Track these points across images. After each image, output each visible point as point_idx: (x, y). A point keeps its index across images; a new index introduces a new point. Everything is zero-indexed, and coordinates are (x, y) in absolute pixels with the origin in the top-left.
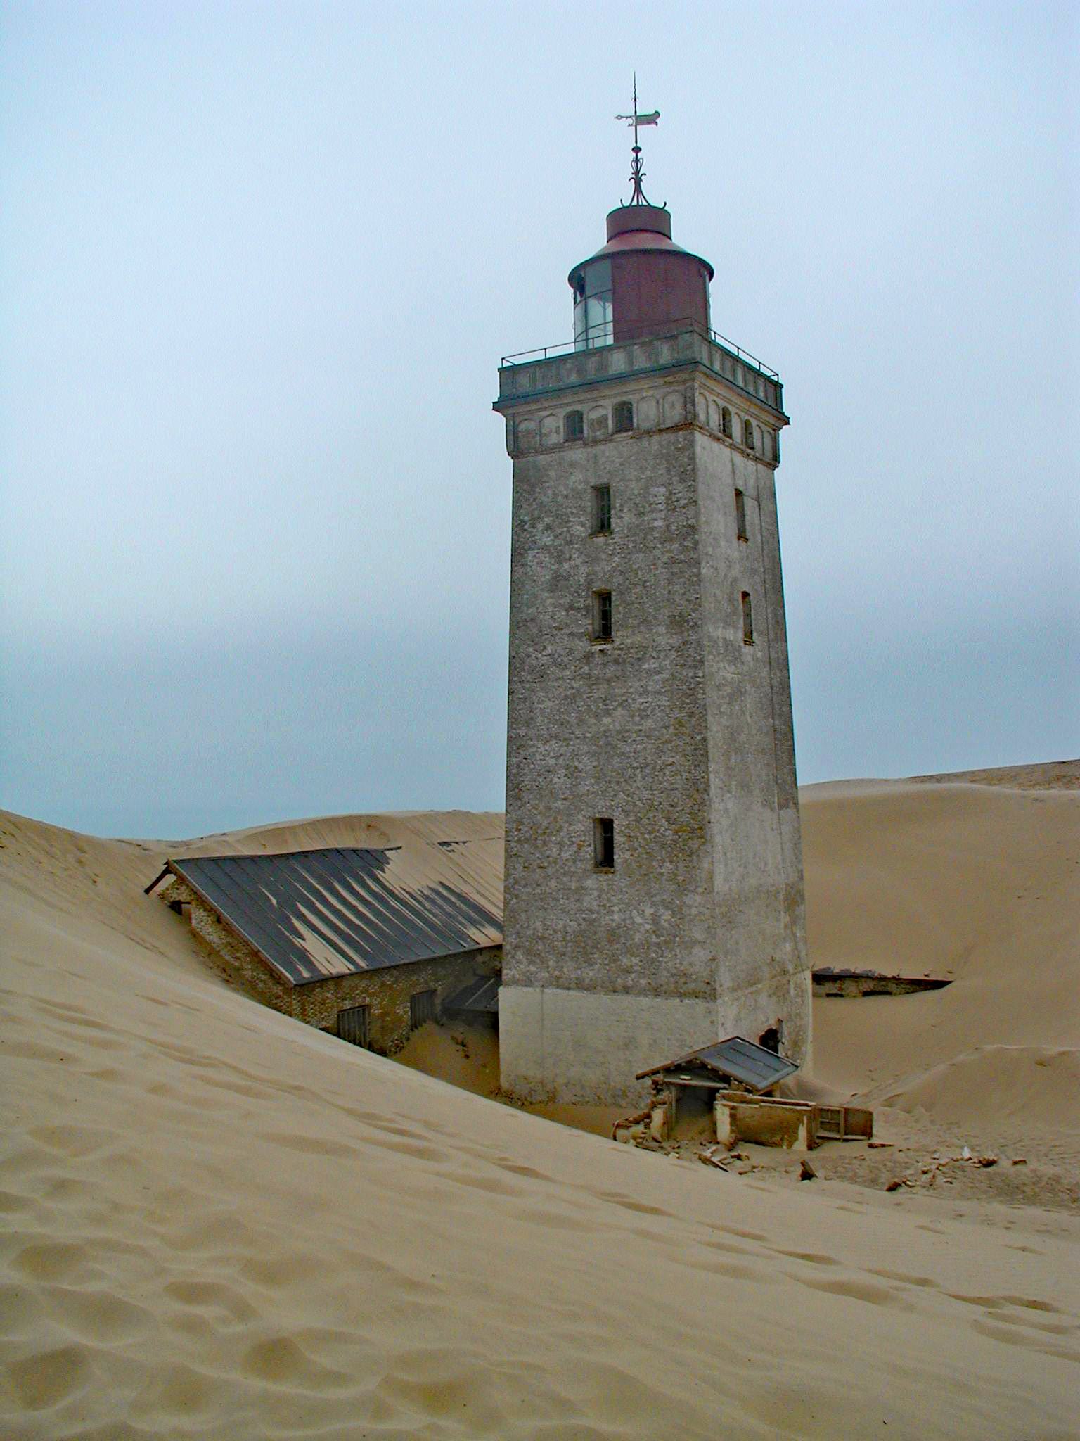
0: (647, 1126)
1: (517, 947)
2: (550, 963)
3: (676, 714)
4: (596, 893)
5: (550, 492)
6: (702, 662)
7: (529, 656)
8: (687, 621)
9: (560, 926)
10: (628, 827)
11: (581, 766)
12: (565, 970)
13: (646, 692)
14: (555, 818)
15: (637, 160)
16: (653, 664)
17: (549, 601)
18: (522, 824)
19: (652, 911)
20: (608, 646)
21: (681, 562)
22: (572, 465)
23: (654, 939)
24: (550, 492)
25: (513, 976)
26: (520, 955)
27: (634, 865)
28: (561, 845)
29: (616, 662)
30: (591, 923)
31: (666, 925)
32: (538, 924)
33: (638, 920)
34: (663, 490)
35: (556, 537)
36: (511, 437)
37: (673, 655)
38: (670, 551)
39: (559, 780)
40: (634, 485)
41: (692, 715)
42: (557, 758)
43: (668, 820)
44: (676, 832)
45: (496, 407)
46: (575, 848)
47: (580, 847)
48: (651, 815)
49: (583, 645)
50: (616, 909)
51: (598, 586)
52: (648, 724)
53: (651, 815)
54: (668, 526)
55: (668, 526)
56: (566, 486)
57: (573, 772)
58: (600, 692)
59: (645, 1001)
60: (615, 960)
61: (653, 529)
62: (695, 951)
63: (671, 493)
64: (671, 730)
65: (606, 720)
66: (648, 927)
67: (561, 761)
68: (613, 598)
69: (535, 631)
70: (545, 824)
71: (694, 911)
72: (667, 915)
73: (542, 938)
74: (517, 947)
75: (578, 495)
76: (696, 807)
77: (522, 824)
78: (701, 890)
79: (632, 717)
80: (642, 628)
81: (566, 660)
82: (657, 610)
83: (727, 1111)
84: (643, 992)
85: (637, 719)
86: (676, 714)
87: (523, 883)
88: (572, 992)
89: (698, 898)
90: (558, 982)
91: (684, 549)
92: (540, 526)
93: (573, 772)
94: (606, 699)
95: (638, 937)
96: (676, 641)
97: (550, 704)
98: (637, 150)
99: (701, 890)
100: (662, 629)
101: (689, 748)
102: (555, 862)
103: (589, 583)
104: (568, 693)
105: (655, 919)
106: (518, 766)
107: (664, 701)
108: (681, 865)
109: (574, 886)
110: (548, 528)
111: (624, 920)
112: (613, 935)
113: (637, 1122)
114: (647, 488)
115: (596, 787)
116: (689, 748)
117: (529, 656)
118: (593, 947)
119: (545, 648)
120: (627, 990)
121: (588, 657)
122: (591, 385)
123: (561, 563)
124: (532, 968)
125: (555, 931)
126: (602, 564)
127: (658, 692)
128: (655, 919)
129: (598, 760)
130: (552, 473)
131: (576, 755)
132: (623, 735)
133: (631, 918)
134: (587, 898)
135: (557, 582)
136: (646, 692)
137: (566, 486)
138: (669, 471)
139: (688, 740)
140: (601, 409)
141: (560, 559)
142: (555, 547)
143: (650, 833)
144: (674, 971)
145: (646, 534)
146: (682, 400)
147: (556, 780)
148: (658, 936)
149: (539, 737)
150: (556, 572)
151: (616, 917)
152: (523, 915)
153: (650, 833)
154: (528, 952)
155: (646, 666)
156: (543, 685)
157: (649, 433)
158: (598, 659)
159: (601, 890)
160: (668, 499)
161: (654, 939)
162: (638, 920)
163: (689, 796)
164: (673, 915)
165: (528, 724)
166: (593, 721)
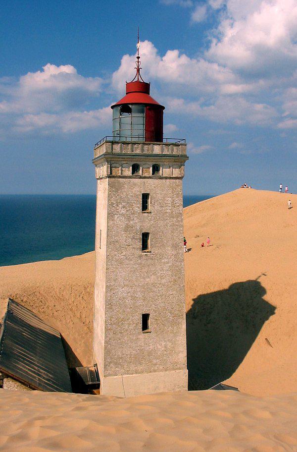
3: (174, 277)
4: (143, 340)
5: (125, 193)
6: (183, 260)
9: (129, 352)
15: (138, 62)
16: (166, 260)
21: (177, 225)
22: (135, 184)
23: (165, 352)
24: (125, 193)
25: (109, 373)
28: (129, 324)
30: (141, 350)
32: (119, 353)
33: (159, 347)
34: (170, 199)
35: (127, 211)
36: (109, 169)
37: (173, 257)
39: (128, 302)
41: (179, 278)
43: (171, 313)
44: (173, 317)
49: (139, 252)
52: (163, 281)
54: (172, 212)
55: (172, 212)
56: (132, 192)
57: (134, 298)
58: (146, 270)
59: (162, 373)
60: (150, 361)
65: (148, 280)
66: (163, 349)
67: (129, 294)
70: (122, 317)
72: (169, 344)
73: (121, 358)
75: (136, 196)
79: (158, 278)
84: (161, 371)
86: (174, 277)
88: (134, 375)
89: (181, 337)
90: (128, 373)
91: (178, 221)
92: (120, 206)
93: (134, 298)
96: (174, 252)
103: (141, 230)
105: (166, 347)
106: (111, 296)
107: (170, 273)
110: (124, 207)
112: (150, 354)
114: (164, 198)
120: (155, 371)
121: (140, 257)
124: (117, 369)
126: (146, 223)
128: (166, 347)
130: (126, 186)
132: (154, 285)
133: (157, 347)
135: (127, 228)
137: (132, 192)
138: (173, 193)
139: (178, 286)
141: (129, 219)
142: (127, 215)
143: (164, 317)
145: (164, 214)
149: (119, 286)
150: (127, 224)
154: (116, 364)
157: (166, 178)
162: (159, 347)
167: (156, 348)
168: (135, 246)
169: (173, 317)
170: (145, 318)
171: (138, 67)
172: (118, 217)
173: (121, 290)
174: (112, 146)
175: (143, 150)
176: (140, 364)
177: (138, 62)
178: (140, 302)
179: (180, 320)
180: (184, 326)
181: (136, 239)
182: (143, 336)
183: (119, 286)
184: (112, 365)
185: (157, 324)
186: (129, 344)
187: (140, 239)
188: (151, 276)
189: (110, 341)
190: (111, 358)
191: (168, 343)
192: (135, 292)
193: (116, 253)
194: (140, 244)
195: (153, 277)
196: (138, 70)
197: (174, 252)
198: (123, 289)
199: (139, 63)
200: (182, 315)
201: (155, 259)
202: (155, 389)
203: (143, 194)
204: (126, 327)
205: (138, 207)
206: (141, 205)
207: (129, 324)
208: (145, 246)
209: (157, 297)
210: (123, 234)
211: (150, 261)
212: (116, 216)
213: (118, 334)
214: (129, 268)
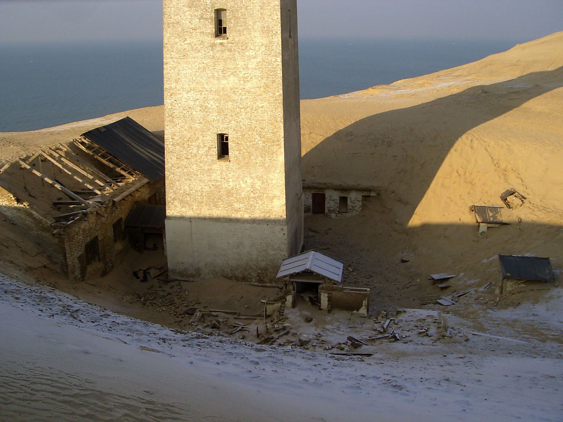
0: (283, 303)
1: (174, 199)
2: (194, 207)
4: (219, 172)
7: (176, 44)
9: (199, 188)
10: (237, 138)
11: (209, 106)
12: (202, 210)
14: (195, 133)
17: (187, 13)
18: (175, 135)
19: (251, 181)
20: (225, 41)
23: (252, 195)
26: (176, 203)
27: (241, 158)
28: (199, 147)
29: (231, 51)
30: (217, 187)
31: (259, 188)
32: (186, 187)
33: (243, 185)
37: (263, 48)
39: (197, 114)
43: (260, 136)
44: (264, 142)
46: (206, 149)
47: (210, 148)
48: (250, 133)
49: (210, 39)
50: (231, 180)
51: (217, 7)
52: (248, 86)
53: (250, 133)
57: (204, 109)
58: (220, 67)
62: (275, 201)
64: (262, 89)
65: (224, 82)
66: (249, 189)
67: (197, 102)
69: (180, 29)
70: (189, 135)
71: (274, 182)
72: (258, 184)
73: (189, 194)
74: (174, 199)
76: (276, 130)
77: (175, 135)
78: (278, 171)
80: (245, 33)
81: (199, 47)
82: (254, 23)
83: (326, 295)
85: (242, 82)
86: (264, 81)
87: (176, 166)
89: (276, 175)
93: (204, 109)
94: (224, 70)
95: (243, 194)
96: (265, 41)
97: (190, 71)
99: (278, 171)
100: (257, 34)
101: (272, 99)
102: (195, 156)
104: (201, 66)
107: (258, 73)
108: (267, 159)
109: (206, 168)
111: (236, 185)
112: (229, 193)
113: (276, 301)
115: (218, 117)
116: (272, 99)
117: (176, 44)
118: (218, 199)
119: (186, 40)
121: (213, 46)
124: (184, 209)
125: (196, 191)
128: (252, 187)
129: (220, 103)
131: (206, 100)
132: (234, 90)
134: (215, 174)
136: (247, 68)
143: (250, 142)
144: (264, 211)
148: (255, 194)
151: (231, 184)
152: (177, 183)
154: (181, 202)
155: (247, 54)
156: (185, 60)
158: (219, 48)
159: (222, 171)
161: (252, 195)
162: (243, 185)
163: (272, 124)
164: (263, 183)
165: (177, 81)
166: (216, 82)
167: (238, 186)
168: (204, 30)
173: (185, 96)
176: (216, 206)
178: (213, 116)
179: (275, 148)
180: (281, 159)
181: (206, 19)
183: (183, 89)
184: (176, 203)
185: (240, 150)
186: (200, 176)
187: (211, 18)
188: (229, 76)
189: (173, 168)
190: (175, 192)
191: (256, 181)
192: (206, 100)
193: (177, 40)
194: (211, 28)
195: (232, 78)
197: (265, 41)
198: (188, 95)
200: (278, 141)
201: (234, 50)
202: (238, 246)
204: (195, 151)
207: (199, 147)
208: (221, 31)
209: (238, 110)
213: (183, 160)
214: (196, 64)
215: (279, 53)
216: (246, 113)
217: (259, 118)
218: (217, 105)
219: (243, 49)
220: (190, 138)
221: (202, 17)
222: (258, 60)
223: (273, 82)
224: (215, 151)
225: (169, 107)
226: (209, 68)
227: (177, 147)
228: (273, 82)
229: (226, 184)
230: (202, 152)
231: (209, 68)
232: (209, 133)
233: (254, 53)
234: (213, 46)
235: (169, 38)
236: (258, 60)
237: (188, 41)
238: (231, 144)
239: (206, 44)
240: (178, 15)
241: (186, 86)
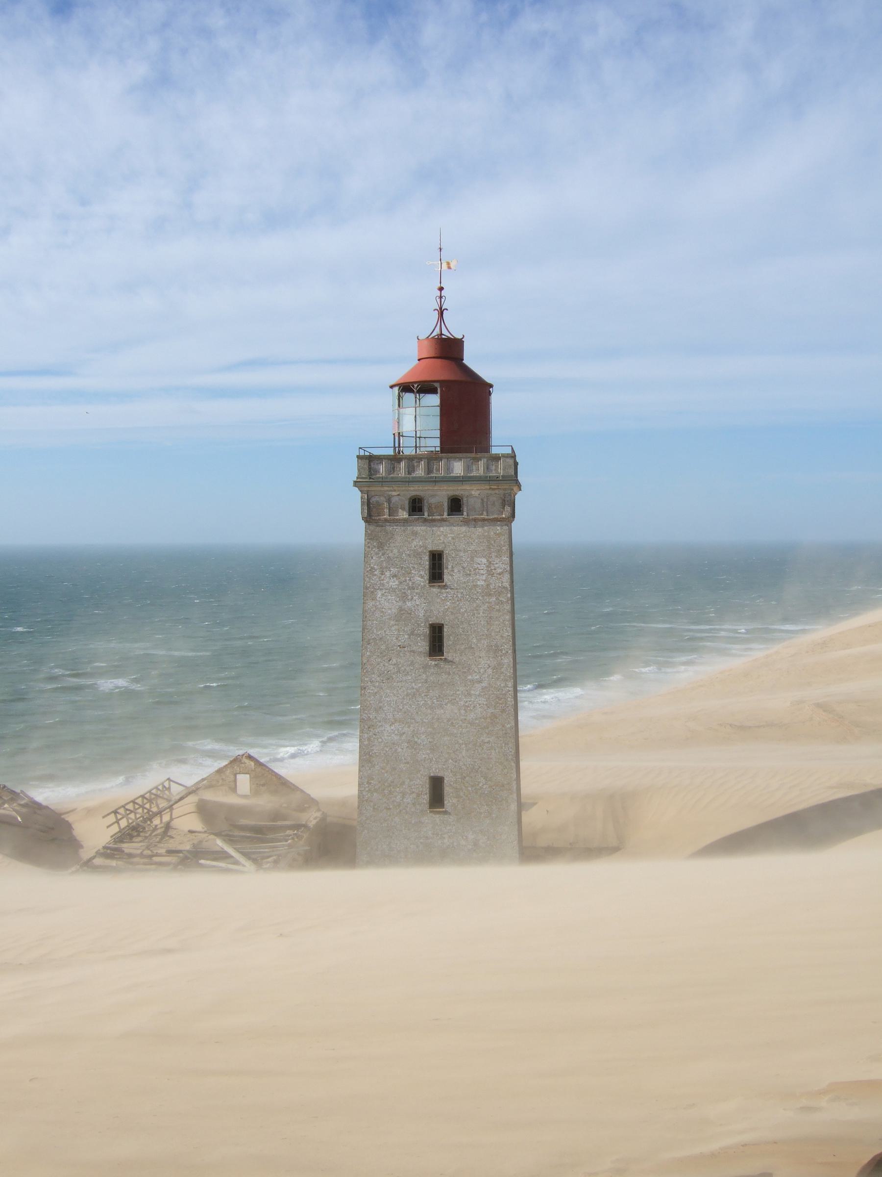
8: (501, 650)
13: (470, 695)
15: (441, 297)
17: (393, 628)
18: (373, 779)
24: (395, 551)
28: (404, 794)
29: (449, 674)
34: (484, 560)
35: (401, 583)
36: (366, 507)
37: (490, 671)
38: (489, 603)
40: (462, 554)
42: (402, 735)
44: (491, 787)
45: (356, 483)
46: (414, 795)
47: (418, 795)
50: (446, 836)
51: (433, 620)
52: (472, 716)
54: (488, 585)
61: (476, 586)
63: (490, 563)
65: (439, 712)
67: (404, 737)
68: (445, 630)
69: (383, 647)
75: (417, 555)
77: (373, 779)
85: (463, 712)
86: (491, 710)
92: (388, 574)
97: (395, 698)
98: (441, 289)
100: (483, 654)
102: (399, 805)
106: (369, 739)
107: (482, 701)
108: (494, 807)
110: (395, 576)
114: (472, 559)
115: (431, 756)
122: (436, 481)
123: (405, 602)
127: (479, 695)
135: (402, 615)
136: (470, 695)
140: (440, 496)
141: (404, 597)
146: (500, 501)
147: (400, 750)
151: (446, 841)
153: (472, 786)
155: (470, 677)
160: (487, 567)
162: (463, 842)
165: (376, 710)
169: (491, 787)
170: (437, 785)
171: (441, 308)
172: (383, 595)
174: (370, 465)
175: (429, 470)
177: (441, 297)
182: (431, 819)
194: (423, 645)
196: (441, 313)
199: (443, 300)
203: (430, 552)
205: (421, 576)
206: (427, 572)
207: (404, 794)
210: (393, 625)
211: (444, 676)
212: (379, 594)
215: (510, 677)
216: (467, 751)
217: (485, 756)
218: (430, 740)
219: (465, 672)
220: (393, 782)
221: (412, 633)
222: (483, 685)
223: (503, 711)
224: (426, 798)
225: (366, 743)
226: (420, 695)
227: (375, 794)
228: (503, 711)
229: (439, 842)
230: (409, 799)
231: (420, 695)
232: (419, 775)
233: (478, 677)
234: (426, 667)
235: (370, 656)
236: (483, 685)
237: (394, 661)
238: (447, 790)
239: (417, 666)
240: (381, 628)
241: (390, 716)
